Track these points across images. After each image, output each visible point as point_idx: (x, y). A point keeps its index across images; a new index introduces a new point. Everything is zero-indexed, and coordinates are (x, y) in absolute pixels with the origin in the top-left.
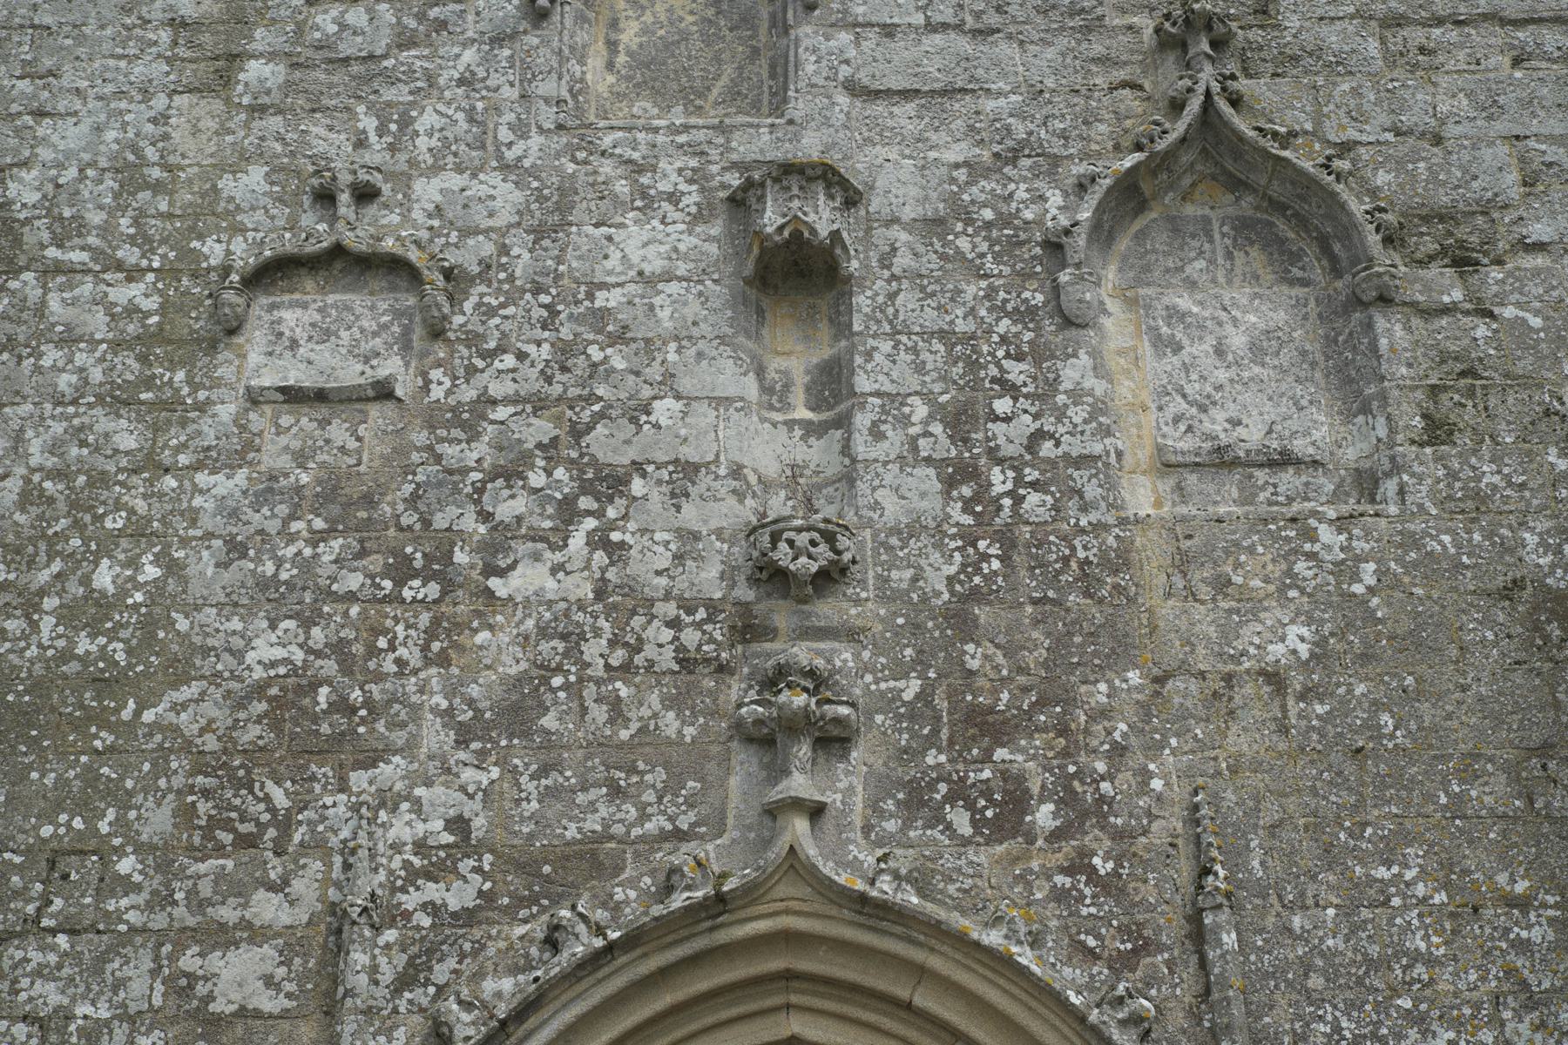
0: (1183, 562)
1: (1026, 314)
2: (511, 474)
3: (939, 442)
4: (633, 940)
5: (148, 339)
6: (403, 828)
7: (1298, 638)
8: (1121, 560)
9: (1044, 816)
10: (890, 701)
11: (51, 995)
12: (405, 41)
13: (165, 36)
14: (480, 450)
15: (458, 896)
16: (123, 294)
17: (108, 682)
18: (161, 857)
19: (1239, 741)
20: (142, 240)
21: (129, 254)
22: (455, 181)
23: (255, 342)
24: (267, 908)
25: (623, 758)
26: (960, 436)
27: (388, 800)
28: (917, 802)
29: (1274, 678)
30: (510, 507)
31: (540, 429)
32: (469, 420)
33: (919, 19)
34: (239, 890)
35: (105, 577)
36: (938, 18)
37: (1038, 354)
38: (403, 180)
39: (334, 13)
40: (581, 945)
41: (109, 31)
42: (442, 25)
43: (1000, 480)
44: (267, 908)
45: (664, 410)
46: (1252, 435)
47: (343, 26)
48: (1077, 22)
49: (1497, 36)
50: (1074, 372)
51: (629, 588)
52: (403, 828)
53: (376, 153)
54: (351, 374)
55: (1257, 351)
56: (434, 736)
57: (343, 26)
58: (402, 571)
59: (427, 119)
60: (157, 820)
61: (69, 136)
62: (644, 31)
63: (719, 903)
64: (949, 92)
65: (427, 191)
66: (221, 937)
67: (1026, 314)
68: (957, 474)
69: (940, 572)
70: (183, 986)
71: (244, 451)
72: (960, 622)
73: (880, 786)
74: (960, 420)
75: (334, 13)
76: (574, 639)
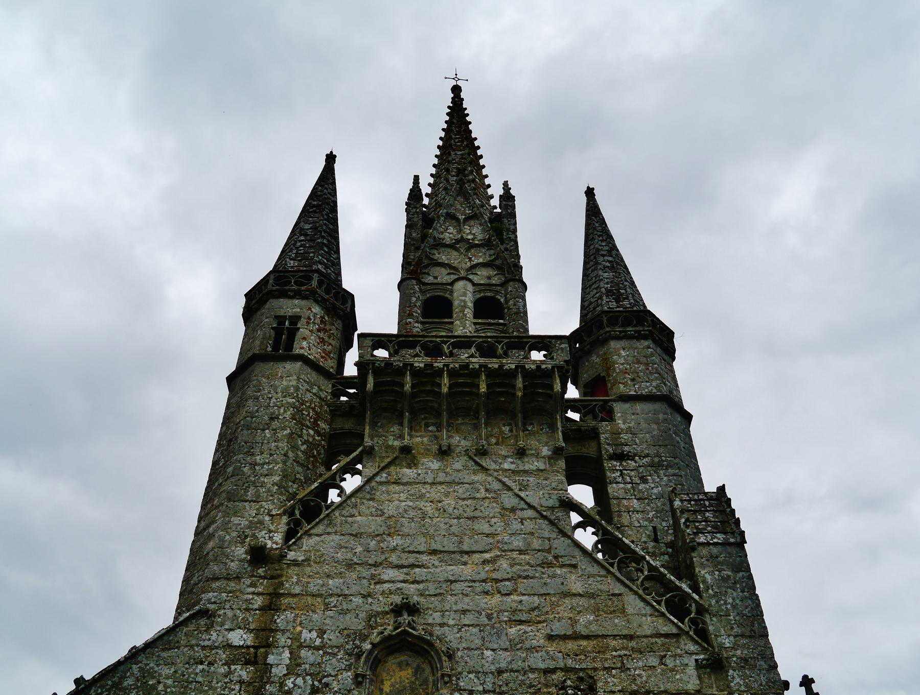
13: (237, 687)
33: (481, 688)
36: (487, 688)
39: (292, 680)
41: (219, 685)
42: (327, 685)
47: (295, 685)
48: (532, 690)
57: (295, 685)
62: (392, 685)
75: (292, 680)
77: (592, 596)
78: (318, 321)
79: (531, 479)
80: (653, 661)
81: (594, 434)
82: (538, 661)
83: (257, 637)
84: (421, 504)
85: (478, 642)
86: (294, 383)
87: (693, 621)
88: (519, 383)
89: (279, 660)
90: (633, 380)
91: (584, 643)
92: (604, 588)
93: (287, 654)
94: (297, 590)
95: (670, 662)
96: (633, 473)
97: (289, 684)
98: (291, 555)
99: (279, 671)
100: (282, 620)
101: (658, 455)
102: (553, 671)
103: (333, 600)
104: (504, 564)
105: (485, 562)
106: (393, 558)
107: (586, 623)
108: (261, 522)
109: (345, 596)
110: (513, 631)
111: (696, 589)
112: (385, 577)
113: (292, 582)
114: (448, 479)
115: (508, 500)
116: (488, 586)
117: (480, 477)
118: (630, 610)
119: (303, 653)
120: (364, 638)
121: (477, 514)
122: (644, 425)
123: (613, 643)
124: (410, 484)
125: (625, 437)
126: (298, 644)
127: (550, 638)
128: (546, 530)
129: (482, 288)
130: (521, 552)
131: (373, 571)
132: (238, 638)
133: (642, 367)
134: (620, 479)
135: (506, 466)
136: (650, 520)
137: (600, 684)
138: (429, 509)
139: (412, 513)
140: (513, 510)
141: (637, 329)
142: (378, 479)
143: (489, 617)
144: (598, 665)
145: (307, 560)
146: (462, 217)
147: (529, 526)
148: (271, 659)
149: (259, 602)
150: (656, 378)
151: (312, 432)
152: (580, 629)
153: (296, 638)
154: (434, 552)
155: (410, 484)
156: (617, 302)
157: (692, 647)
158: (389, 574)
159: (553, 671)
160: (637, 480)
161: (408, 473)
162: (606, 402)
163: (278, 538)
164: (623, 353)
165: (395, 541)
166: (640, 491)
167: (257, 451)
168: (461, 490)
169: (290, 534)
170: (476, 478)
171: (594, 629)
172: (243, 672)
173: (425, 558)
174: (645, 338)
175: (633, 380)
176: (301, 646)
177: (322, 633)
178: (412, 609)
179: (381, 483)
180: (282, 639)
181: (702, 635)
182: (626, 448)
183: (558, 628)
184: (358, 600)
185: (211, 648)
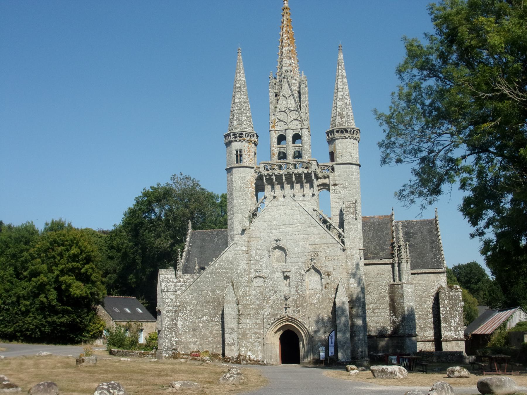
0: (309, 297)
1: (301, 280)
2: (270, 291)
3: (295, 289)
4: (279, 319)
5: (248, 282)
6: (266, 313)
7: (316, 301)
8: (306, 296)
9: (301, 312)
10: (292, 305)
11: (249, 322)
12: (261, 259)
14: (268, 290)
15: (269, 317)
16: (246, 279)
17: (249, 305)
18: (253, 315)
19: (312, 308)
20: (246, 275)
21: (246, 276)
22: (265, 270)
23: (254, 282)
24: (259, 317)
25: (278, 309)
26: (297, 288)
27: (265, 311)
28: (294, 311)
29: (314, 304)
30: (270, 293)
31: (272, 288)
32: (267, 288)
34: (258, 316)
35: (248, 298)
37: (302, 282)
38: (262, 270)
40: (276, 320)
43: (299, 291)
44: (259, 317)
45: (279, 287)
46: (315, 287)
49: (332, 258)
50: (304, 284)
51: (278, 298)
52: (266, 313)
53: (260, 268)
54: (260, 285)
55: (315, 281)
56: (267, 308)
58: (265, 298)
59: (263, 265)
60: (253, 313)
61: (241, 267)
63: (283, 317)
64: (297, 263)
65: (263, 271)
66: (257, 319)
67: (301, 280)
68: (297, 291)
69: (295, 297)
70: (256, 322)
71: (255, 290)
72: (296, 301)
73: (292, 310)
74: (297, 287)
76: (275, 302)
77: (320, 234)
78: (247, 149)
79: (307, 203)
80: (331, 249)
81: (328, 177)
82: (307, 250)
83: (248, 248)
84: (280, 212)
85: (294, 247)
86: (244, 175)
87: (342, 240)
88: (303, 176)
89: (253, 253)
90: (341, 156)
91: (316, 245)
92: (322, 232)
93: (254, 252)
94: (254, 236)
95: (334, 249)
96: (337, 190)
97: (256, 257)
98: (251, 228)
99: (253, 255)
100: (252, 243)
101: (345, 184)
102: (310, 252)
103: (262, 238)
104: (300, 227)
105: (296, 227)
106: (274, 227)
107: (317, 241)
108: (243, 220)
109: (265, 237)
110: (301, 243)
111: (343, 231)
112: (273, 232)
113: (253, 234)
114: (286, 204)
115: (301, 210)
116: (296, 233)
117: (294, 203)
118: (327, 237)
119: (258, 251)
120: (270, 247)
121: (294, 214)
122: (342, 173)
123: (323, 245)
124: (277, 206)
125: (337, 178)
126: (256, 250)
127: (310, 245)
128: (310, 218)
129: (295, 130)
130: (304, 224)
131: (270, 231)
132: (244, 248)
133: (345, 150)
134: (334, 193)
135: (300, 199)
136: (340, 205)
137: (319, 255)
138: (282, 213)
139: (278, 215)
140: (302, 212)
141: (344, 135)
142: (269, 205)
143: (296, 241)
144: (319, 251)
145: (255, 229)
146: (287, 96)
147: (306, 216)
148: (251, 253)
149: (246, 240)
150: (348, 155)
151: (251, 189)
152: (316, 242)
153: (256, 248)
154: (284, 225)
155: (277, 206)
156: (341, 119)
157: (340, 246)
158: (274, 231)
159: (310, 252)
160: (338, 193)
161: (276, 203)
162: (332, 165)
163: (248, 223)
164: (339, 145)
165: (274, 223)
166: (339, 196)
167: (238, 199)
168: (289, 207)
169: (251, 222)
170: (293, 203)
171: (319, 242)
172: (246, 256)
173: (282, 226)
174: (347, 138)
175: (341, 156)
176: (257, 250)
177: (261, 246)
178: (280, 240)
179: (270, 206)
180: (253, 248)
181: (343, 242)
182: (337, 182)
183: (311, 243)
184: (267, 238)
185: (239, 251)
